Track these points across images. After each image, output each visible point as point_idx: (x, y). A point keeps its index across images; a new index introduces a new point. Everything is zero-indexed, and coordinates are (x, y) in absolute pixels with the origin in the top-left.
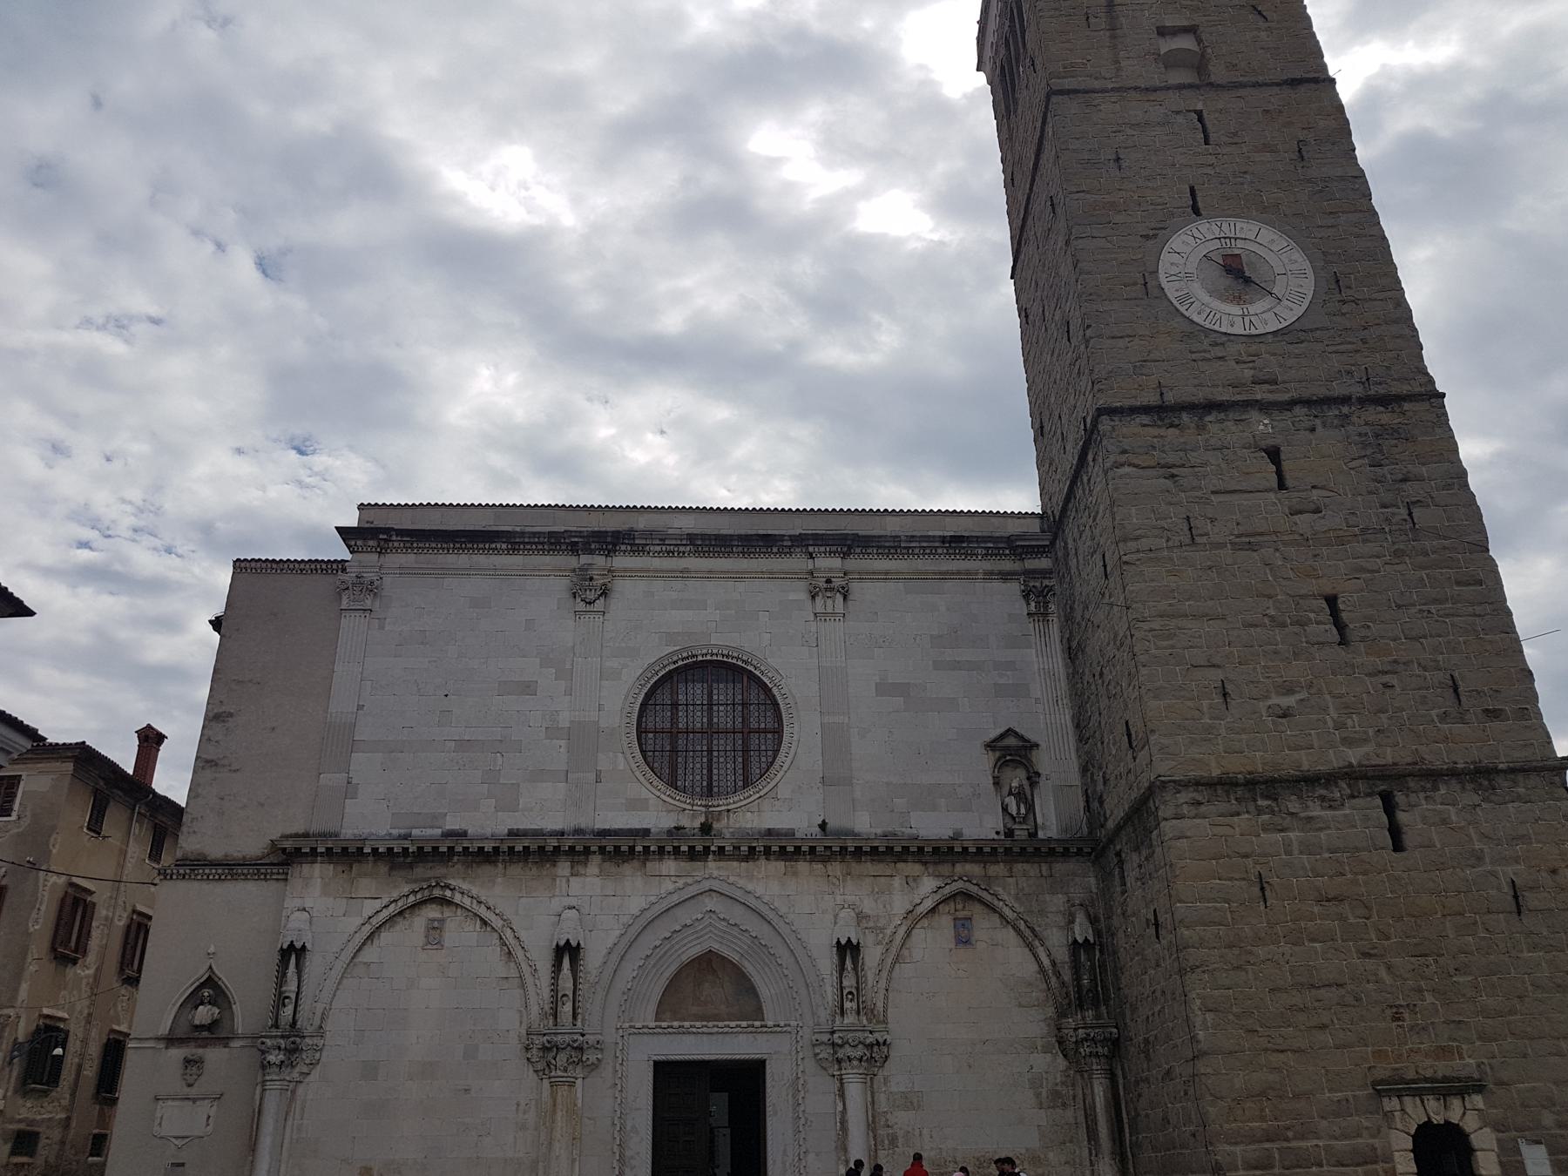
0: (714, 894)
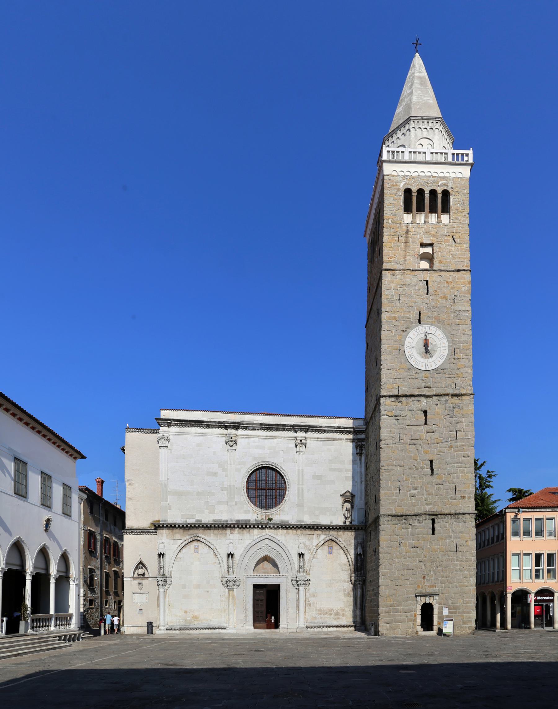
0: (267, 539)
